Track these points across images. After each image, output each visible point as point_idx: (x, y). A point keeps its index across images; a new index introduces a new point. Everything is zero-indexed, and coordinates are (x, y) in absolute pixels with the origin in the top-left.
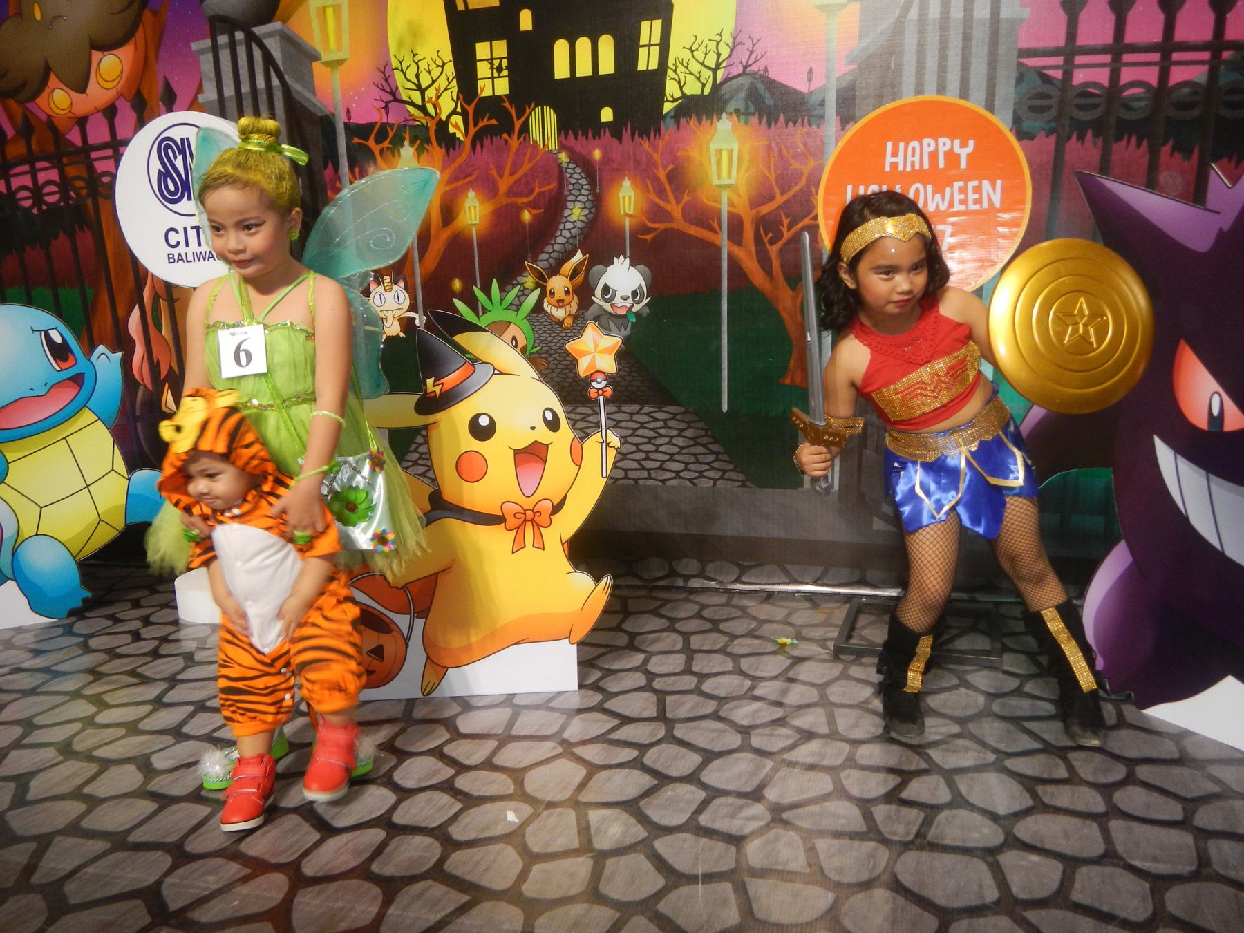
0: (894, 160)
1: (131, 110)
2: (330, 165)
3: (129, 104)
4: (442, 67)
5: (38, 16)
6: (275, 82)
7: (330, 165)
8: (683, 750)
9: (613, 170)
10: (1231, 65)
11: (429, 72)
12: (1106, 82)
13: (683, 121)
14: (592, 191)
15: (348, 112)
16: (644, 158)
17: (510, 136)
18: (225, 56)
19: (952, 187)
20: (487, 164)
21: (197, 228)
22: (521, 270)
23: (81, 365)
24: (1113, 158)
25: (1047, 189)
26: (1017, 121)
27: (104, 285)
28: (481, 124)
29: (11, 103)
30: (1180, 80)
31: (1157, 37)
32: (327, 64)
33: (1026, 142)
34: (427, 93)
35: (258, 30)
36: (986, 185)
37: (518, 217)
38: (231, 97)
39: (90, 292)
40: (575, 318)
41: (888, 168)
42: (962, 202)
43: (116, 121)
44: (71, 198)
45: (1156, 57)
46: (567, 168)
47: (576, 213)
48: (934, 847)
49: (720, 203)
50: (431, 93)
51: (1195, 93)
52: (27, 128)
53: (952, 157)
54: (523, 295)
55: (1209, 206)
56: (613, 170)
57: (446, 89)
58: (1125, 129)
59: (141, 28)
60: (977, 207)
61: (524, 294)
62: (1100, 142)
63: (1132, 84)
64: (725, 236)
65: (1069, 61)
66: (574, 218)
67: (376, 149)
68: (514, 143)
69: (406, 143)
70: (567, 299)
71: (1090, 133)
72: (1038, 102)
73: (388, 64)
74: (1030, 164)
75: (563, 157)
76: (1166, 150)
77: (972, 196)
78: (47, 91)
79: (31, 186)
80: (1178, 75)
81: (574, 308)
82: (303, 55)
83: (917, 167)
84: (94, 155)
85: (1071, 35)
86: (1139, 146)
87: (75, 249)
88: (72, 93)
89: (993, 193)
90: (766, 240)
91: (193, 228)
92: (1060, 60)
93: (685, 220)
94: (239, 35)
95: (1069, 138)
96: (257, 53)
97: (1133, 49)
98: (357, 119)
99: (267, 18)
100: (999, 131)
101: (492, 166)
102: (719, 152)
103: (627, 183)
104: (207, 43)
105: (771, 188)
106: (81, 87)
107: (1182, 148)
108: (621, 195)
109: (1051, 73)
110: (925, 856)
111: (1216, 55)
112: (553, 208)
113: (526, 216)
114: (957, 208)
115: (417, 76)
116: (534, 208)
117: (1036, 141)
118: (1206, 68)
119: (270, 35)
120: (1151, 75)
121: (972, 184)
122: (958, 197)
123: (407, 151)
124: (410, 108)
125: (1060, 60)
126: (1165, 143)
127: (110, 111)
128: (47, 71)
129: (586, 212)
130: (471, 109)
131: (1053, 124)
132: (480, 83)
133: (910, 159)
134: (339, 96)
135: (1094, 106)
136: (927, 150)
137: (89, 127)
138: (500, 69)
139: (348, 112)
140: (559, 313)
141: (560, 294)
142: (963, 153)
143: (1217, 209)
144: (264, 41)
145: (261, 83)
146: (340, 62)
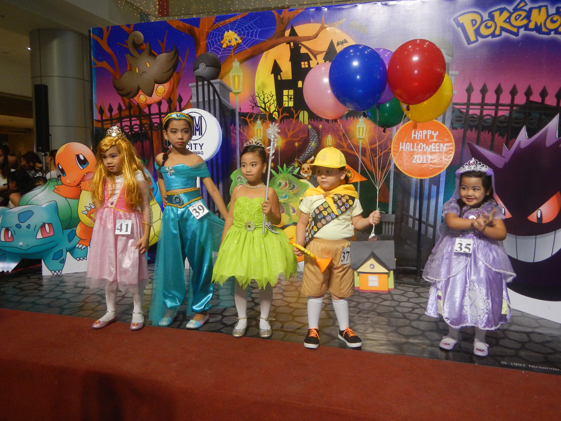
0: (415, 136)
1: (167, 103)
2: (233, 124)
3: (166, 101)
4: (272, 97)
5: (137, 72)
6: (217, 98)
7: (233, 124)
8: (351, 301)
9: (325, 132)
10: (516, 111)
11: (268, 98)
12: (479, 114)
13: (349, 118)
14: (318, 138)
15: (240, 108)
16: (336, 128)
17: (293, 119)
18: (200, 89)
19: (431, 144)
20: (285, 127)
21: (195, 144)
22: (294, 161)
23: (154, 185)
24: (481, 136)
25: (461, 145)
26: (452, 124)
27: (152, 160)
28: (283, 115)
29: (125, 98)
30: (501, 115)
31: (494, 102)
32: (234, 93)
33: (455, 131)
34: (267, 104)
35: (212, 81)
36: (441, 144)
37: (294, 144)
38: (201, 102)
39: (146, 161)
40: (311, 177)
41: (412, 138)
42: (434, 149)
43: (161, 106)
44: (143, 130)
45: (494, 107)
46: (311, 130)
47: (313, 144)
48: (421, 321)
49: (359, 143)
50: (268, 104)
51: (505, 119)
52: (130, 107)
53: (432, 137)
54: (294, 169)
55: (503, 155)
56: (325, 132)
57: (273, 104)
58: (484, 128)
59: (172, 78)
60: (439, 151)
61: (294, 169)
62: (477, 132)
63: (487, 115)
64: (360, 154)
65: (468, 107)
66: (312, 146)
67: (248, 121)
68: (294, 121)
69: (259, 119)
70: (308, 171)
71: (474, 129)
72: (458, 119)
73: (254, 95)
74: (454, 139)
75: (310, 127)
76: (497, 134)
77: (437, 148)
78: (138, 95)
79: (129, 125)
80: (500, 113)
81: (310, 174)
82: (226, 90)
83: (421, 138)
84: (152, 117)
85: (469, 99)
86: (488, 133)
87: (143, 146)
88: (146, 96)
89: (444, 147)
90: (373, 156)
91: (194, 144)
92: (465, 107)
93: (348, 148)
94: (206, 82)
95: (468, 130)
96: (211, 88)
97: (487, 105)
98: (244, 111)
99: (216, 78)
100: (446, 130)
101: (286, 128)
102: (360, 128)
103: (330, 136)
104: (195, 84)
105: (376, 140)
106: (151, 96)
107: (501, 135)
108: (328, 139)
109: (462, 110)
110: (418, 322)
111: (512, 108)
112: (305, 142)
113: (297, 144)
114: (433, 151)
115: (264, 99)
116: (299, 142)
117: (457, 130)
118: (509, 112)
119: (216, 83)
120: (493, 113)
121: (437, 144)
122: (433, 148)
123: (259, 122)
124: (260, 108)
125: (465, 107)
126: (496, 133)
127: (159, 103)
128: (139, 89)
129: (316, 144)
130: (281, 110)
131: (463, 126)
132: (284, 102)
133: (419, 136)
134: (237, 104)
135: (476, 121)
136: (424, 134)
137: (151, 108)
138: (291, 98)
139: (240, 108)
140: (306, 175)
141: (306, 169)
142: (435, 135)
143: (504, 156)
144: (214, 85)
145: (212, 98)
146: (239, 93)
